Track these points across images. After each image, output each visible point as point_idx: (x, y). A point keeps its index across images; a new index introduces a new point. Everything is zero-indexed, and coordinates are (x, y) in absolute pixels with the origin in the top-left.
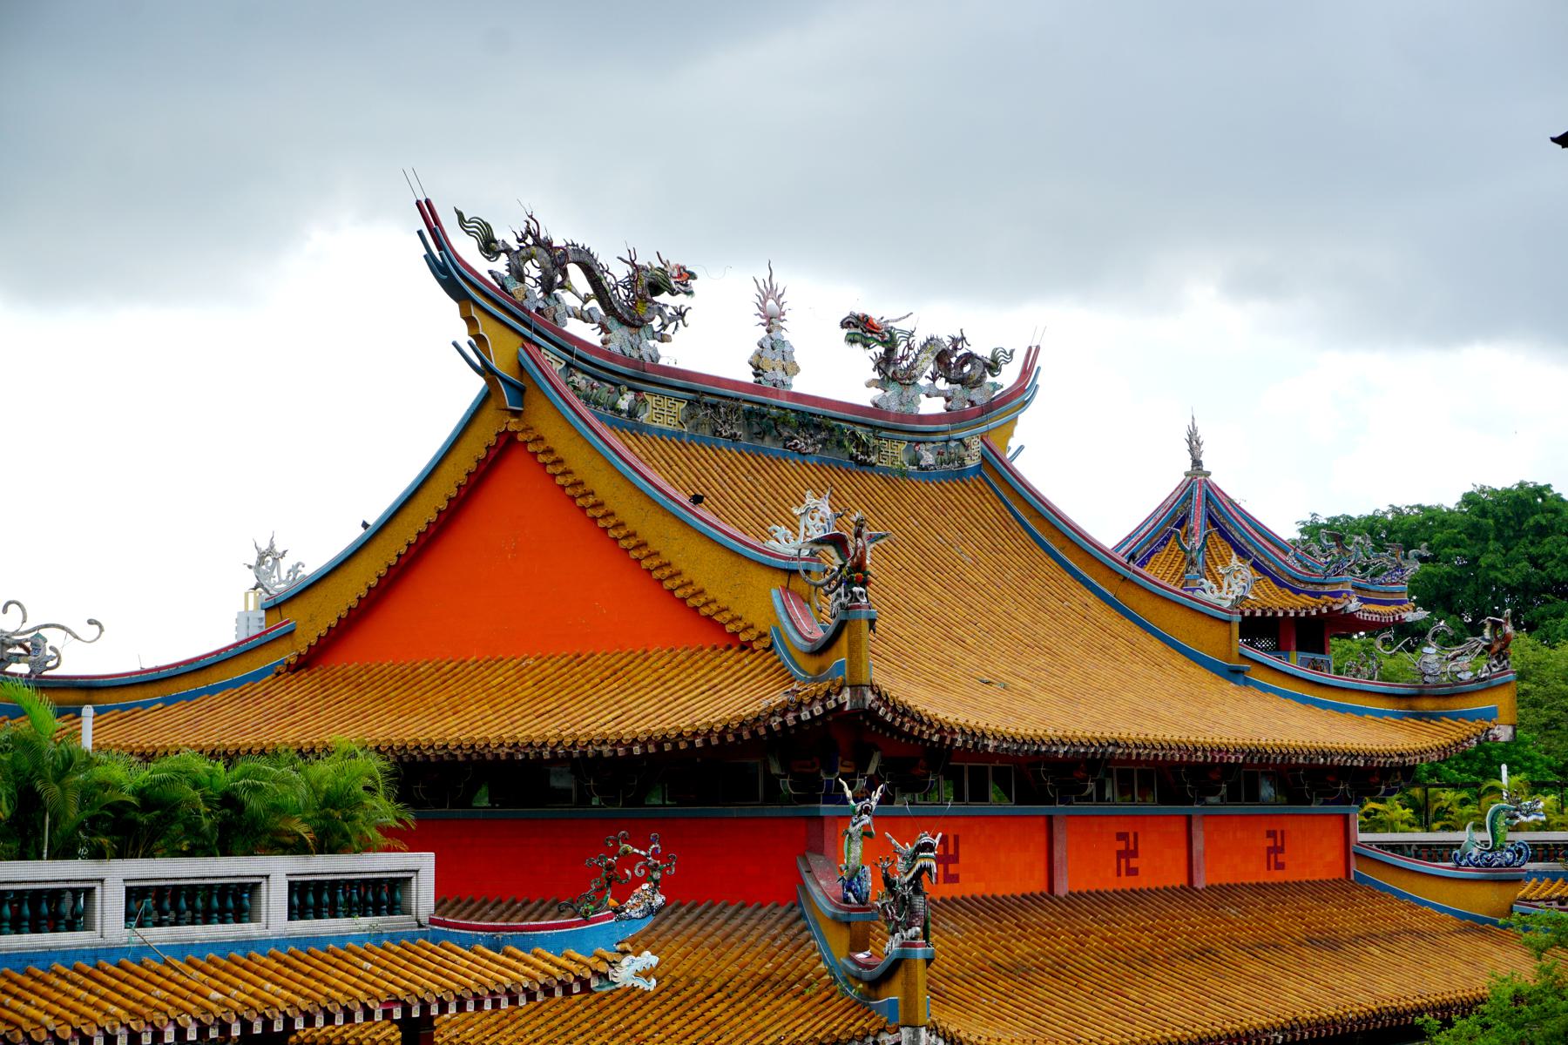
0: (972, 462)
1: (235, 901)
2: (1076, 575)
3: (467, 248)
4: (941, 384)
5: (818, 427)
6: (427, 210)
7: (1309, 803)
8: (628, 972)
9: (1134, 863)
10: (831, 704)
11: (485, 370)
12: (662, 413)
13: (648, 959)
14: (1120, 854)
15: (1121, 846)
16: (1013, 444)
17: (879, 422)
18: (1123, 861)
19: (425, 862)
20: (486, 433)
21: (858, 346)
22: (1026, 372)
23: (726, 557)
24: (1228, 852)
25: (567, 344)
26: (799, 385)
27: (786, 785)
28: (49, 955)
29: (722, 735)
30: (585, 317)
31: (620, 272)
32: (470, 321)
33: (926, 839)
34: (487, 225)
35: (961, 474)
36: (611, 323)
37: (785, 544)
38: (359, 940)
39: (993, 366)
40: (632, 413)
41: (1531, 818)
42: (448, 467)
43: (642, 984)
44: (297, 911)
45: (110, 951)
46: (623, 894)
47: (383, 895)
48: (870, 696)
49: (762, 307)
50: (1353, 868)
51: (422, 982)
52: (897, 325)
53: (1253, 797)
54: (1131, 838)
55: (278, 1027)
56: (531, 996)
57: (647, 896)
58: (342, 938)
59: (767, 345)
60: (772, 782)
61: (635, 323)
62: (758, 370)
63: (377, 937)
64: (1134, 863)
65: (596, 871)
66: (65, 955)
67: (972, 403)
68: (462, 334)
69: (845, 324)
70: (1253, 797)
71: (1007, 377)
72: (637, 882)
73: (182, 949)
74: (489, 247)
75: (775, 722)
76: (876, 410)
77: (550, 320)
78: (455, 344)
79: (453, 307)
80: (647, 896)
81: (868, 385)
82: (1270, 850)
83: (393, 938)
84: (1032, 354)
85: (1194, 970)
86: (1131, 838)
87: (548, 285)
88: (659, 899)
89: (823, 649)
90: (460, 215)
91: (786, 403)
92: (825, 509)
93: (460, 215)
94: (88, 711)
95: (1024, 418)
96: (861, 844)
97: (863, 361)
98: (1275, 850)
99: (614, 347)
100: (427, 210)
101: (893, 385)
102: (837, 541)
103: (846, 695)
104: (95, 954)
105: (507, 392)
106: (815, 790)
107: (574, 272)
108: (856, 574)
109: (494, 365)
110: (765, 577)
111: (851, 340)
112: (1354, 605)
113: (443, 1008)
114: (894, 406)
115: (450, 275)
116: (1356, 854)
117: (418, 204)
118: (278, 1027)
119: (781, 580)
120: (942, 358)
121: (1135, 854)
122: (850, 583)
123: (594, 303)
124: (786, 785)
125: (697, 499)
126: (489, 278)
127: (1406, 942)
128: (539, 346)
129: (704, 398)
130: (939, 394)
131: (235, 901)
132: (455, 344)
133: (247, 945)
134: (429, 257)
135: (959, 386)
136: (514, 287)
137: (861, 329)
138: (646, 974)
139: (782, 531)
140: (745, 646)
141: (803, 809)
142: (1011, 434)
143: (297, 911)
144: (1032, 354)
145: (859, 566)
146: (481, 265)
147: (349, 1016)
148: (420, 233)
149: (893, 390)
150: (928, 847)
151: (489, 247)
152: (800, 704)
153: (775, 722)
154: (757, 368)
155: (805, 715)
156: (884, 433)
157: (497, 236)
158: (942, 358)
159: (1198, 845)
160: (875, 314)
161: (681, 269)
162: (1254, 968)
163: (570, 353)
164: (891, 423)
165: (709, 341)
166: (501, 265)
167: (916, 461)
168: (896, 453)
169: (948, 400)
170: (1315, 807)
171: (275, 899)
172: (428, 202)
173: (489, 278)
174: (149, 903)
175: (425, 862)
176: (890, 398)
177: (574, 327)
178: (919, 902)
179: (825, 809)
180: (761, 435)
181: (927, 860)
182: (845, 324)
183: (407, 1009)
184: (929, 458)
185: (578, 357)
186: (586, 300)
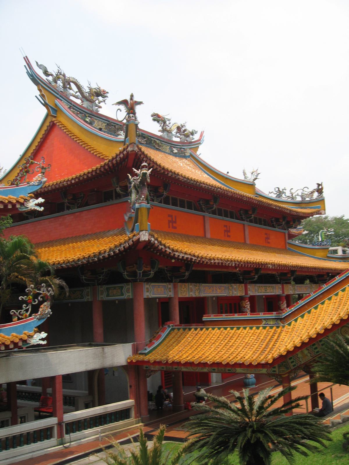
3: (40, 72)
4: (178, 134)
5: (145, 138)
6: (26, 59)
7: (275, 227)
9: (229, 234)
11: (45, 105)
14: (225, 231)
17: (161, 140)
18: (226, 233)
21: (156, 122)
25: (70, 102)
30: (77, 97)
32: (40, 90)
34: (45, 67)
36: (83, 99)
39: (192, 134)
43: (38, 208)
50: (288, 247)
52: (166, 117)
61: (92, 102)
64: (229, 234)
67: (187, 141)
68: (38, 93)
69: (152, 116)
74: (46, 73)
76: (160, 137)
78: (36, 96)
79: (35, 87)
81: (159, 131)
86: (228, 227)
87: (64, 87)
90: (37, 63)
93: (37, 63)
95: (200, 147)
100: (26, 59)
101: (165, 132)
105: (53, 112)
107: (73, 86)
109: (47, 102)
111: (154, 120)
114: (166, 137)
115: (35, 79)
116: (288, 243)
117: (24, 58)
120: (179, 128)
123: (78, 94)
126: (46, 80)
128: (61, 100)
130: (178, 137)
132: (36, 96)
134: (28, 72)
135: (183, 136)
137: (157, 118)
142: (197, 150)
146: (44, 77)
148: (25, 66)
149: (165, 133)
151: (46, 73)
156: (163, 143)
157: (49, 71)
158: (179, 128)
160: (161, 114)
161: (104, 91)
163: (71, 104)
164: (165, 141)
166: (50, 78)
170: (277, 229)
172: (26, 57)
173: (46, 80)
176: (165, 135)
182: (152, 116)
185: (73, 105)
186: (76, 92)
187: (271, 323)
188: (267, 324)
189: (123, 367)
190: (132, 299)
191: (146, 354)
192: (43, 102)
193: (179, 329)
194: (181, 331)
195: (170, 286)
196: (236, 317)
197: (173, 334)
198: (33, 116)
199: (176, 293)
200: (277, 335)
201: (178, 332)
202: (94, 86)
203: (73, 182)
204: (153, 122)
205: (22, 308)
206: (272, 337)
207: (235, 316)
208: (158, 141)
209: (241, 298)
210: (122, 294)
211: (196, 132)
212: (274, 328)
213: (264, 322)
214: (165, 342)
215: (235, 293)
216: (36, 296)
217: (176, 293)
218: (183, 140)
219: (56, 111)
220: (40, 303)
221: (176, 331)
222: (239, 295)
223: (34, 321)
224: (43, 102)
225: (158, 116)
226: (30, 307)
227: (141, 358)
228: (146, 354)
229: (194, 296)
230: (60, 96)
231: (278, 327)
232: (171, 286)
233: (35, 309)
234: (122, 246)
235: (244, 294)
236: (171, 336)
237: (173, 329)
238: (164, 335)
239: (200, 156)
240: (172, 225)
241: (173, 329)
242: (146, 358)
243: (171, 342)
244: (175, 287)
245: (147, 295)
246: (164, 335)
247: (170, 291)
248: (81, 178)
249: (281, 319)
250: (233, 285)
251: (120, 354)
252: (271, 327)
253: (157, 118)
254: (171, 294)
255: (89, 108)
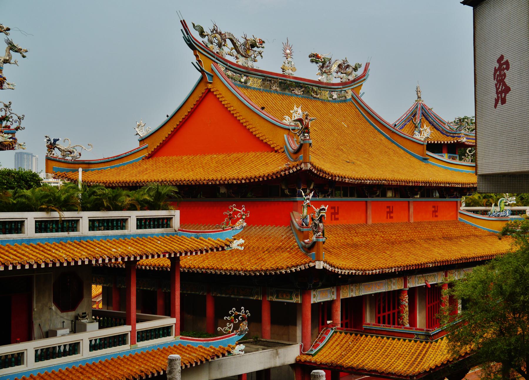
0: (349, 97)
1: (121, 224)
2: (379, 131)
3: (196, 34)
5: (302, 87)
6: (183, 23)
7: (445, 198)
8: (235, 245)
9: (392, 215)
10: (299, 168)
11: (202, 71)
12: (254, 82)
13: (241, 241)
14: (388, 212)
15: (388, 210)
16: (361, 91)
17: (320, 85)
19: (176, 214)
20: (202, 89)
21: (314, 64)
22: (366, 70)
23: (270, 126)
24: (413, 212)
25: (225, 62)
26: (296, 74)
27: (287, 192)
28: (66, 238)
29: (267, 177)
31: (242, 41)
32: (197, 56)
33: (323, 207)
35: (345, 101)
36: (239, 56)
37: (287, 121)
38: (158, 235)
40: (246, 82)
41: (511, 202)
42: (191, 99)
43: (239, 248)
44: (139, 227)
45: (84, 238)
46: (234, 222)
47: (165, 223)
48: (309, 166)
49: (285, 50)
50: (459, 217)
51: (176, 247)
53: (384, 195)
54: (391, 207)
55: (132, 259)
56: (207, 251)
57: (241, 223)
58: (152, 235)
59: (286, 62)
60: (283, 190)
61: (246, 56)
62: (283, 70)
63: (163, 234)
65: (226, 215)
66: (71, 238)
67: (349, 80)
68: (195, 60)
70: (384, 195)
71: (360, 72)
72: (238, 219)
73: (106, 237)
74: (202, 34)
75: (282, 173)
77: (221, 55)
80: (241, 223)
82: (433, 212)
83: (167, 235)
84: (367, 65)
85: (407, 245)
86: (391, 207)
88: (245, 224)
89: (297, 152)
90: (194, 25)
91: (292, 80)
92: (300, 111)
93: (194, 25)
94: (80, 170)
95: (365, 84)
96: (307, 209)
97: (315, 67)
98: (435, 211)
99: (240, 63)
100: (183, 23)
101: (324, 74)
102: (300, 120)
103: (303, 165)
104: (80, 238)
106: (294, 193)
107: (228, 41)
108: (306, 130)
110: (283, 131)
111: (312, 61)
112: (464, 140)
113: (181, 254)
117: (181, 21)
118: (132, 259)
119: (287, 132)
121: (392, 212)
122: (304, 133)
123: (234, 50)
124: (287, 192)
125: (263, 108)
127: (472, 238)
128: (217, 63)
129: (267, 78)
131: (121, 224)
133: (124, 236)
134: (184, 37)
135: (345, 75)
136: (210, 46)
137: (315, 58)
138: (241, 245)
139: (287, 117)
140: (276, 151)
141: (292, 199)
143: (139, 227)
144: (367, 65)
145: (307, 128)
147: (153, 257)
149: (325, 76)
150: (324, 209)
151: (202, 34)
152: (290, 168)
153: (282, 173)
154: (283, 69)
155: (291, 171)
159: (412, 210)
162: (426, 245)
163: (227, 65)
165: (269, 62)
166: (206, 39)
167: (331, 96)
168: (325, 95)
169: (341, 79)
170: (447, 199)
171: (132, 224)
172: (184, 21)
174: (94, 225)
175: (176, 214)
177: (228, 58)
178: (321, 225)
179: (298, 199)
180: (284, 89)
181: (323, 213)
182: (310, 56)
183: (170, 255)
184: (335, 96)
187: (422, 337)
188: (418, 338)
189: (291, 365)
190: (300, 304)
191: (313, 355)
192: (199, 68)
193: (341, 333)
194: (343, 334)
195: (333, 290)
196: (392, 328)
197: (336, 337)
198: (184, 78)
199: (338, 295)
200: (425, 350)
201: (340, 336)
202: (250, 37)
203: (243, 181)
204: (311, 63)
205: (226, 326)
206: (421, 351)
207: (391, 328)
208: (315, 88)
209: (400, 292)
210: (291, 299)
211: (360, 66)
212: (424, 343)
213: (416, 336)
214: (329, 345)
215: (394, 287)
216: (237, 316)
217: (338, 295)
218: (344, 80)
219: (212, 76)
220: (240, 322)
221: (338, 334)
222: (397, 289)
223: (236, 337)
224: (199, 68)
225: (316, 56)
226: (232, 325)
227: (309, 358)
228: (313, 355)
229: (354, 296)
230: (217, 59)
231: (427, 342)
232: (334, 290)
233: (236, 327)
234: (299, 267)
235: (403, 288)
236: (334, 339)
237: (336, 332)
238: (327, 337)
239: (363, 98)
240: (335, 217)
241: (336, 332)
242: (313, 359)
243: (334, 345)
244: (338, 291)
245: (313, 300)
246: (327, 337)
247: (333, 294)
248: (252, 180)
249: (430, 336)
250: (392, 279)
251: (291, 354)
252: (421, 342)
253: (315, 58)
254: (334, 297)
255: (244, 64)
